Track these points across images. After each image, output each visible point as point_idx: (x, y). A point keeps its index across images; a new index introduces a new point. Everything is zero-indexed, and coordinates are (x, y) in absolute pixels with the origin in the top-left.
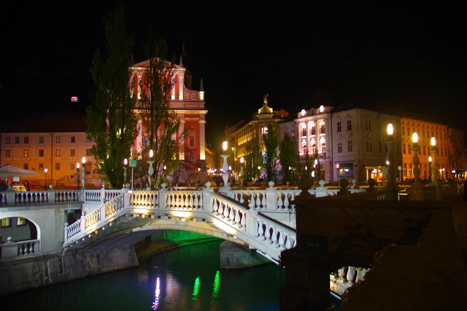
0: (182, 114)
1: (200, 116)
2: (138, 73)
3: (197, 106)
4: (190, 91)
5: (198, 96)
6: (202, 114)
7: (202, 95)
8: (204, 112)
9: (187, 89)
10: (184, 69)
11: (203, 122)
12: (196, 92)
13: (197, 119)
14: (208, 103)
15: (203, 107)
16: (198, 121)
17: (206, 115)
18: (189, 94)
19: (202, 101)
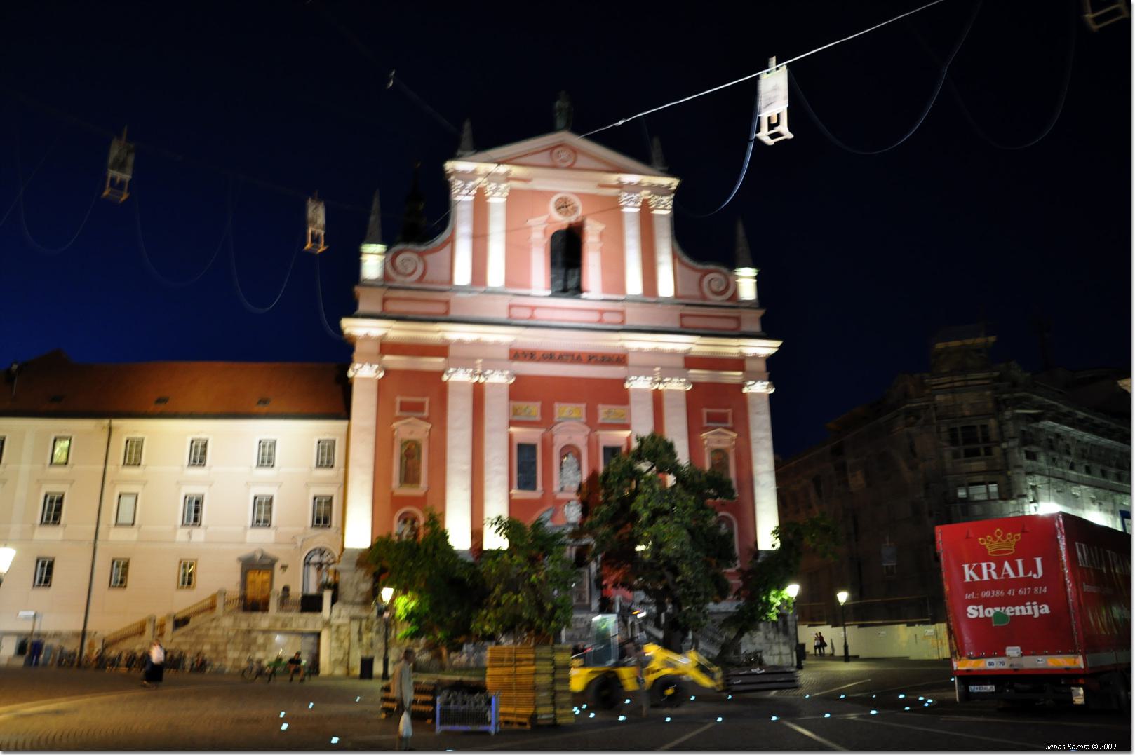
0: (673, 353)
1: (749, 365)
2: (493, 185)
3: (731, 324)
4: (700, 267)
5: (731, 289)
6: (756, 357)
7: (746, 283)
8: (766, 348)
9: (686, 259)
10: (673, 182)
11: (760, 389)
12: (725, 270)
13: (735, 376)
14: (773, 314)
15: (756, 328)
16: (742, 386)
17: (771, 362)
18: (698, 275)
19: (748, 305)
